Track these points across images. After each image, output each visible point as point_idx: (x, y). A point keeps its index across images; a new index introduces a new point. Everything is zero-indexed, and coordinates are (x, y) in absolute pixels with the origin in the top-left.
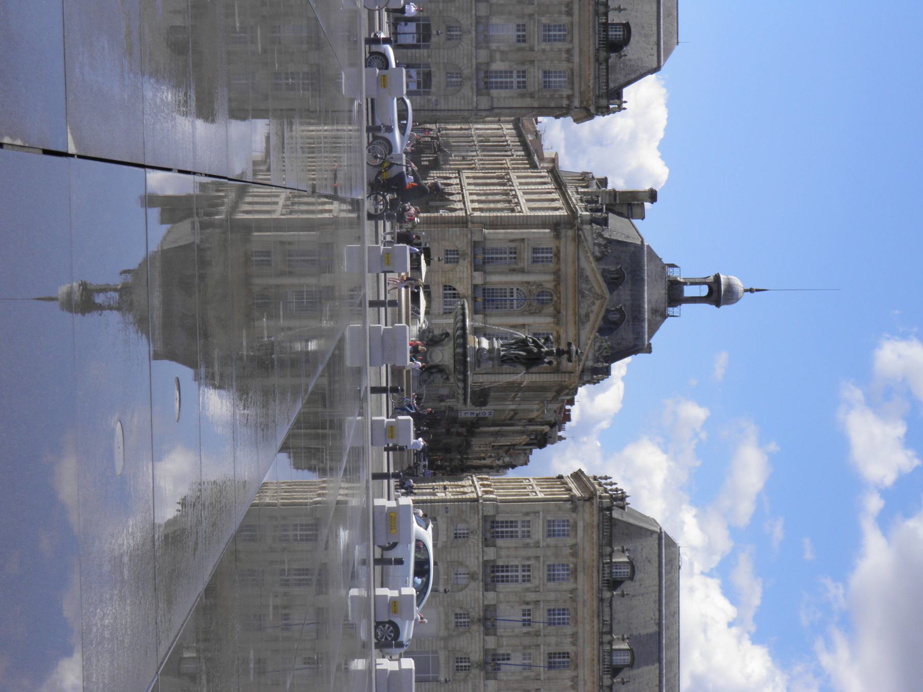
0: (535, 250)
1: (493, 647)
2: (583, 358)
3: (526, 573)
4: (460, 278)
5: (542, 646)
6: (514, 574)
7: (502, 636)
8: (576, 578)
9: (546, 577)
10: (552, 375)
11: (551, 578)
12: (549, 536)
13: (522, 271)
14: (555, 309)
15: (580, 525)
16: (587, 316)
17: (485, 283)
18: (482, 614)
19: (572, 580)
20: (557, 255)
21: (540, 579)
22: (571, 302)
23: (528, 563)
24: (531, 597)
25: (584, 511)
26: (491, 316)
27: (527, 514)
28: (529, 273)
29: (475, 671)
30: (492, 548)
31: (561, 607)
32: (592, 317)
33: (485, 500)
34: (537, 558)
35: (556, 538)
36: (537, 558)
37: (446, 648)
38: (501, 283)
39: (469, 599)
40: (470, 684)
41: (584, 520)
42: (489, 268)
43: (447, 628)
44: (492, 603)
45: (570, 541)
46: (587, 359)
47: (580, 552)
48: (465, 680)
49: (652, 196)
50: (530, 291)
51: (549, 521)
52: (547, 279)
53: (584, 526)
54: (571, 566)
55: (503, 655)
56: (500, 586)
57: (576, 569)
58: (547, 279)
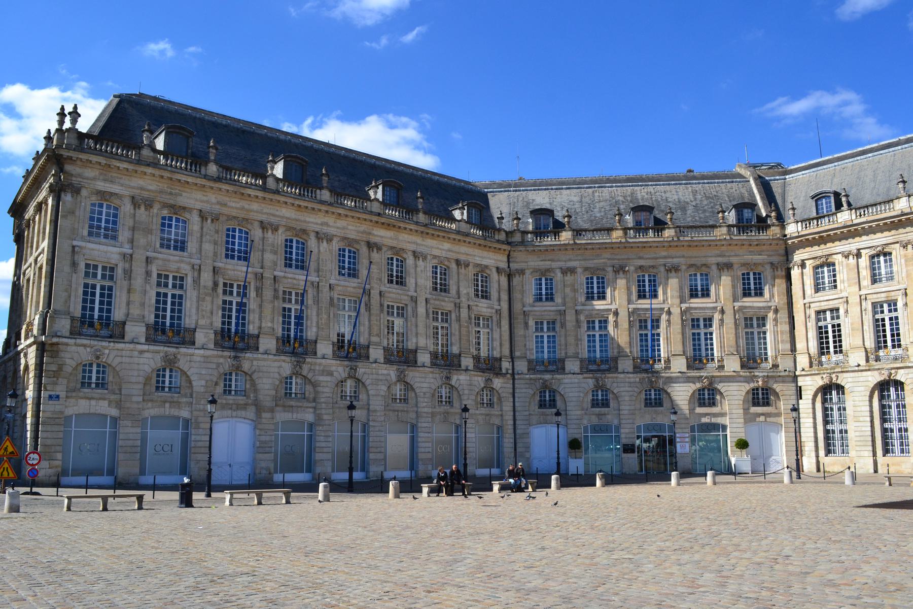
1: (274, 342)
3: (170, 282)
5: (276, 273)
6: (169, 300)
7: (260, 328)
8: (184, 208)
9: (178, 253)
11: (181, 246)
12: (115, 238)
15: (101, 185)
18: (227, 354)
19: (187, 215)
21: (182, 261)
23: (155, 275)
24: (207, 278)
25: (80, 175)
27: (74, 264)
29: (306, 368)
30: (127, 328)
31: (224, 239)
33: (43, 330)
34: (148, 260)
35: (119, 226)
36: (148, 260)
37: (272, 410)
39: (203, 372)
40: (321, 378)
41: (94, 179)
43: (244, 407)
44: (212, 336)
45: (127, 208)
47: (146, 194)
48: (315, 385)
51: (90, 234)
53: (105, 180)
54: (165, 213)
55: (283, 329)
56: (188, 321)
57: (172, 207)
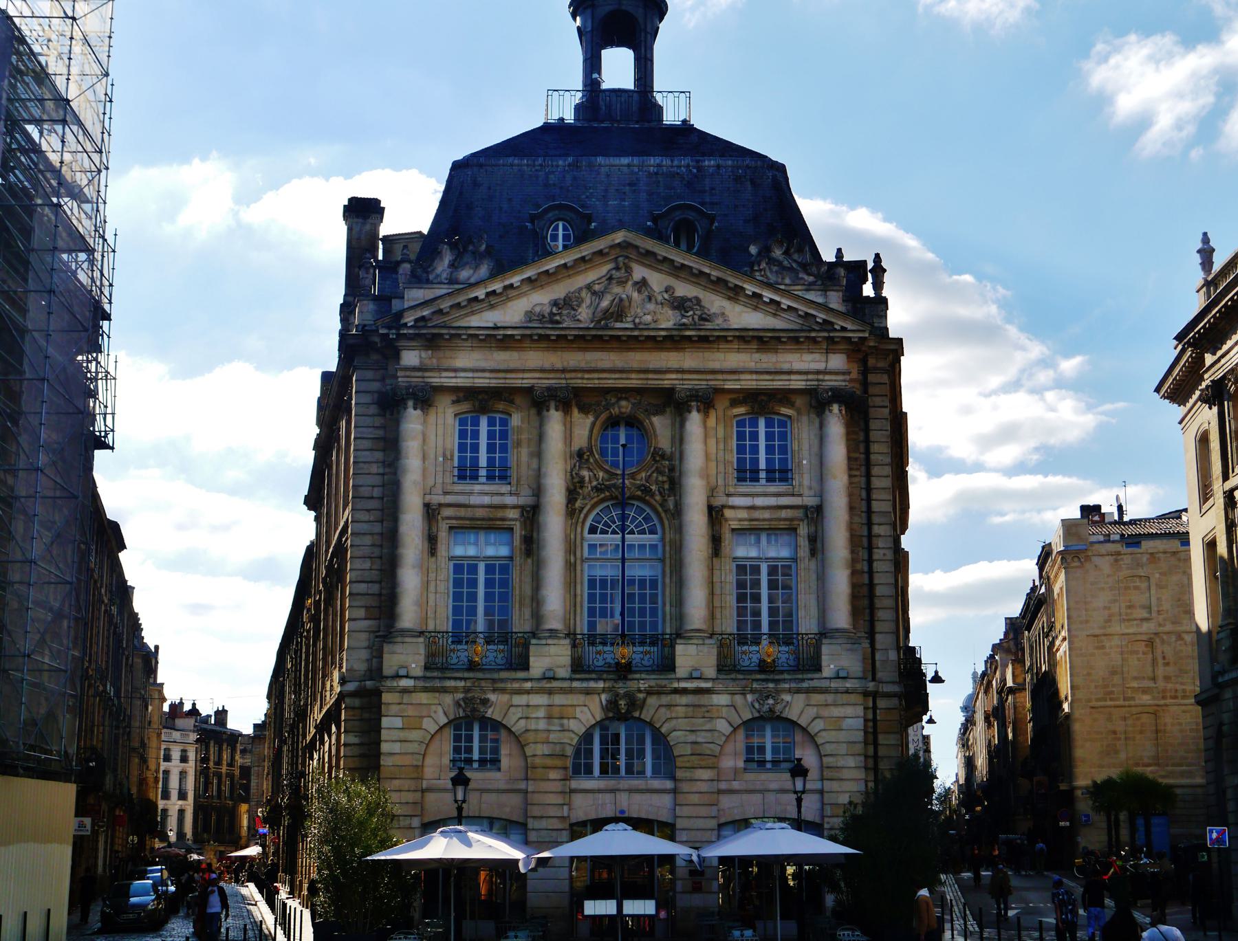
0: (467, 472)
2: (821, 316)
4: (549, 717)
10: (874, 425)
13: (532, 514)
14: (659, 411)
16: (680, 305)
17: (571, 634)
20: (481, 400)
22: (636, 359)
26: (680, 617)
28: (538, 492)
32: (684, 289)
38: (571, 582)
42: (520, 623)
46: (824, 307)
49: (363, 212)
50: (597, 489)
52: (561, 435)
58: (561, 435)
